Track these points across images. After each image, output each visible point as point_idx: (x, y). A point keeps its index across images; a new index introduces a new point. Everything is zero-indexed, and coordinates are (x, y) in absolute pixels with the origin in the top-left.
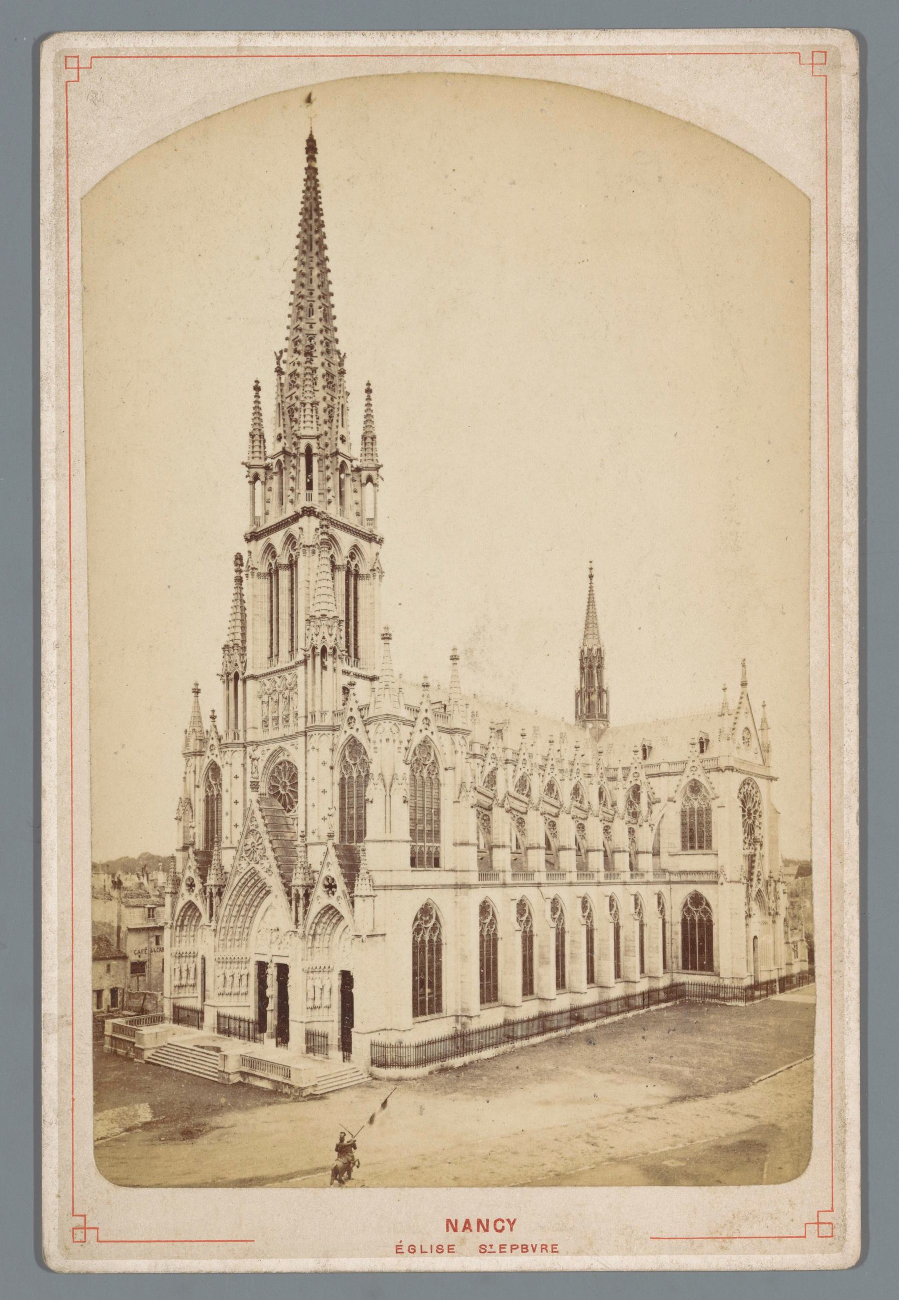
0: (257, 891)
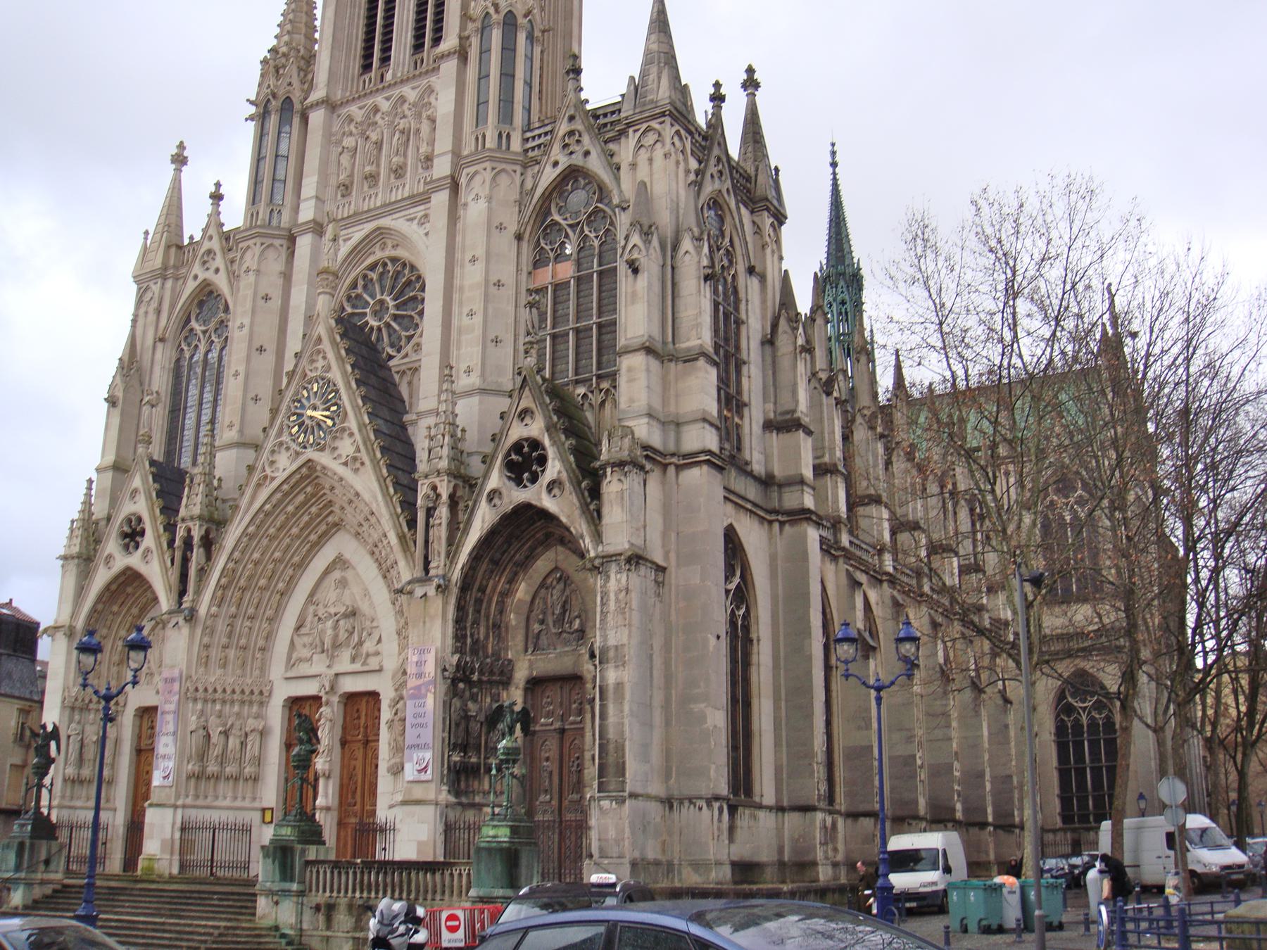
0: (307, 524)
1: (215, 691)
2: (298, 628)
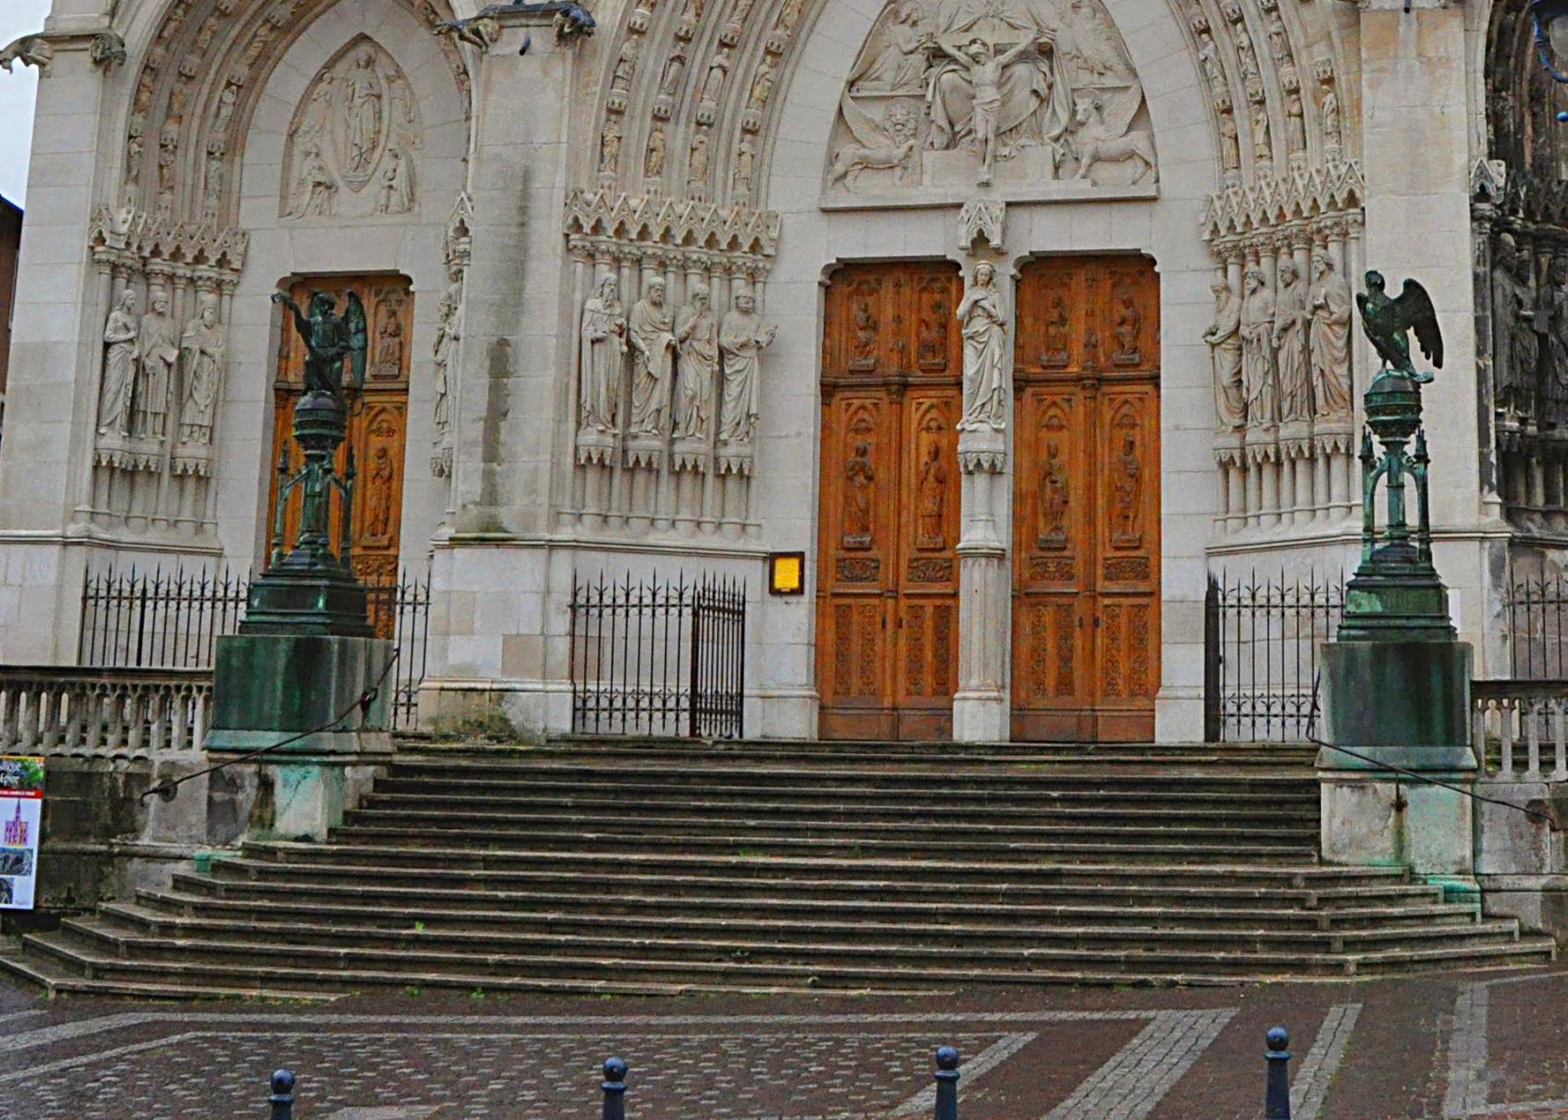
1: (644, 233)
2: (851, 84)
